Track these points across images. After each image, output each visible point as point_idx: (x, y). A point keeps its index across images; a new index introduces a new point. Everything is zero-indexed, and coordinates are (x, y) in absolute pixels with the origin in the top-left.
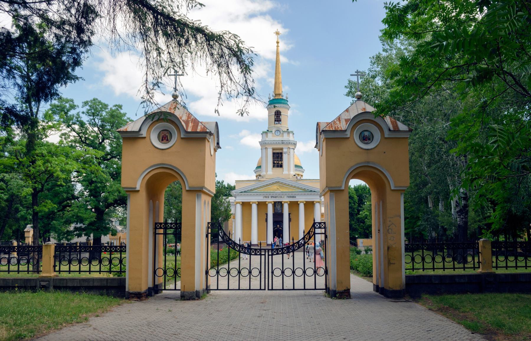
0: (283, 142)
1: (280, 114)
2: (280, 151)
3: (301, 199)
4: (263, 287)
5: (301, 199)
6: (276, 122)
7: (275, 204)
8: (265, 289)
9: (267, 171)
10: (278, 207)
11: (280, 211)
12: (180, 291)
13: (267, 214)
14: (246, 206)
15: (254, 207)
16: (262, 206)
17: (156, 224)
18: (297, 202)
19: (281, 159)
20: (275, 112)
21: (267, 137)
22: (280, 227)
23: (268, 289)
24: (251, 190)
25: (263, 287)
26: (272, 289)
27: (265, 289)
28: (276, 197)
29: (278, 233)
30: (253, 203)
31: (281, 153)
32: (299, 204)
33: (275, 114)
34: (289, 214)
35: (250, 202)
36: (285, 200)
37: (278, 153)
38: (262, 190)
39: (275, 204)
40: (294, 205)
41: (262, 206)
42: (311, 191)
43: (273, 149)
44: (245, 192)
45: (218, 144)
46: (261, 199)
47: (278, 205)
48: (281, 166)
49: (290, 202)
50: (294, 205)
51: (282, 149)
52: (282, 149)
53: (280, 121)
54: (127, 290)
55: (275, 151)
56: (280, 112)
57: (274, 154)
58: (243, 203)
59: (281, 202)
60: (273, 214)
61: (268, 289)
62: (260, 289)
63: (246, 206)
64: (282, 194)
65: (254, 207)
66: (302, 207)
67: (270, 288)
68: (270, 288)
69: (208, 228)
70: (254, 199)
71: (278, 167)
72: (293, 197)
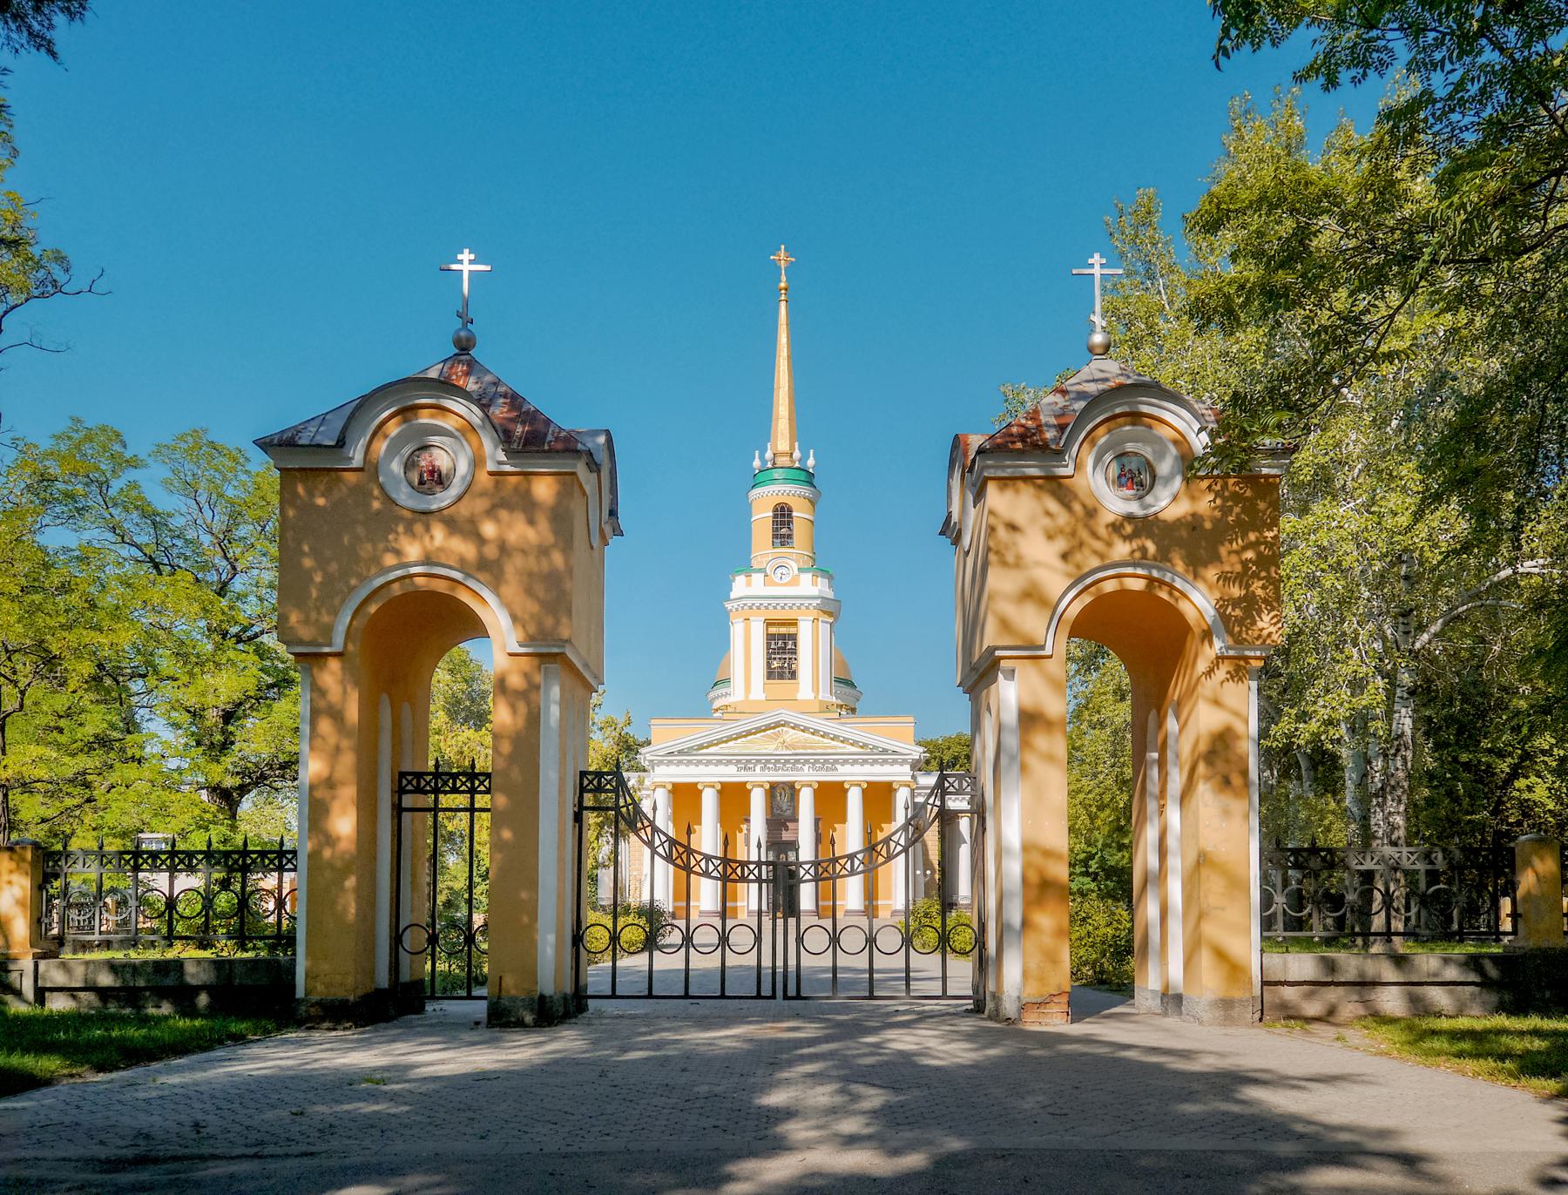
1: (790, 516)
2: (792, 630)
4: (766, 991)
5: (855, 774)
7: (773, 790)
8: (773, 997)
12: (484, 1004)
16: (733, 798)
17: (402, 775)
20: (775, 510)
21: (749, 584)
23: (786, 997)
24: (701, 747)
25: (766, 991)
26: (798, 997)
27: (773, 997)
31: (793, 637)
33: (775, 516)
34: (817, 821)
36: (806, 777)
37: (783, 637)
39: (773, 790)
40: (831, 798)
41: (733, 798)
42: (885, 751)
44: (680, 752)
45: (613, 513)
46: (731, 774)
47: (781, 800)
48: (793, 675)
50: (831, 798)
51: (793, 623)
52: (794, 623)
53: (790, 536)
54: (300, 993)
55: (773, 630)
56: (790, 510)
57: (770, 638)
58: (675, 785)
59: (791, 785)
61: (786, 997)
62: (759, 996)
66: (854, 800)
67: (792, 992)
68: (792, 992)
69: (583, 790)
70: (708, 775)
71: (781, 677)
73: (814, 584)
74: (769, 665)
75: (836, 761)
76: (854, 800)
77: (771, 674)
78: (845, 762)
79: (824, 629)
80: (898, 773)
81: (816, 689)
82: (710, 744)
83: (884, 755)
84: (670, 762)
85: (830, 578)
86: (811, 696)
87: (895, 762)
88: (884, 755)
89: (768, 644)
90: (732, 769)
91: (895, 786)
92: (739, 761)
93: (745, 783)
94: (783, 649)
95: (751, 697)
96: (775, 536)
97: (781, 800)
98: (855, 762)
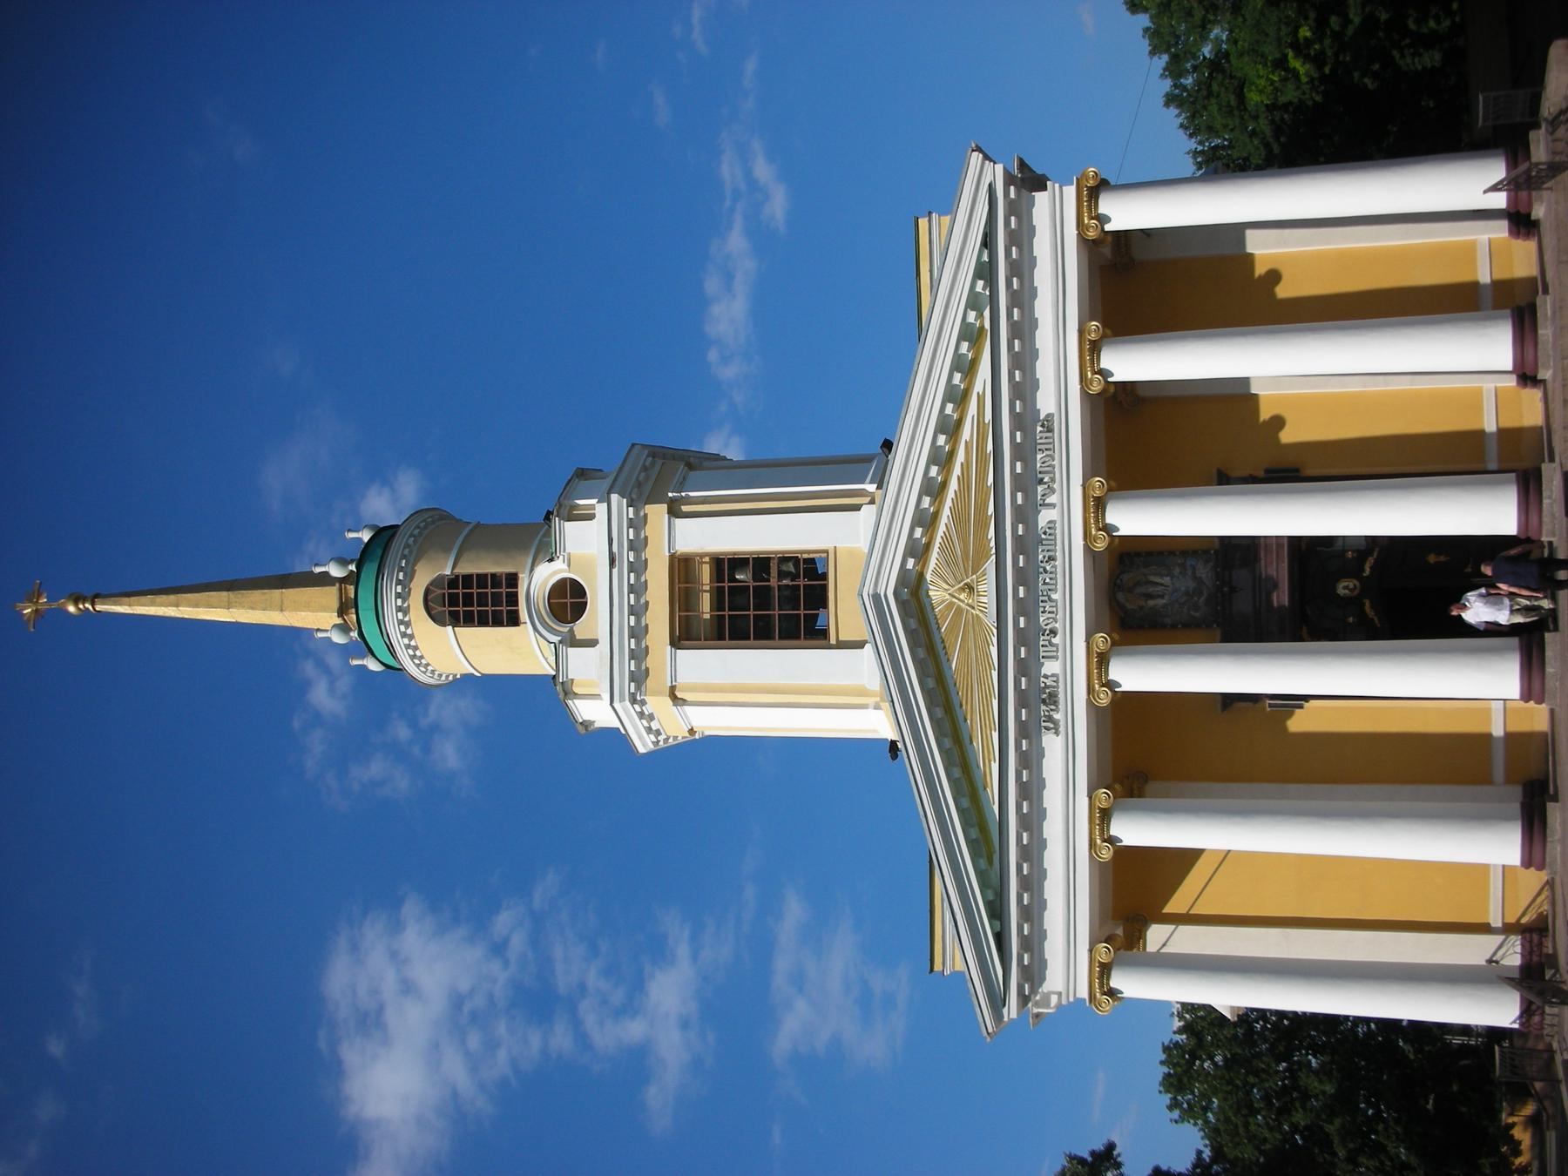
0: (630, 556)
1: (453, 582)
10: (1168, 586)
11: (1204, 571)
20: (437, 619)
22: (1356, 573)
29: (1405, 594)
31: (726, 565)
33: (456, 620)
38: (984, 744)
42: (986, 271)
43: (685, 635)
44: (997, 911)
46: (1066, 758)
47: (1146, 595)
51: (682, 567)
52: (682, 567)
75: (1018, 422)
78: (1025, 390)
84: (1027, 944)
85: (582, 474)
92: (1024, 730)
96: (498, 622)
97: (1146, 595)
98: (1025, 360)
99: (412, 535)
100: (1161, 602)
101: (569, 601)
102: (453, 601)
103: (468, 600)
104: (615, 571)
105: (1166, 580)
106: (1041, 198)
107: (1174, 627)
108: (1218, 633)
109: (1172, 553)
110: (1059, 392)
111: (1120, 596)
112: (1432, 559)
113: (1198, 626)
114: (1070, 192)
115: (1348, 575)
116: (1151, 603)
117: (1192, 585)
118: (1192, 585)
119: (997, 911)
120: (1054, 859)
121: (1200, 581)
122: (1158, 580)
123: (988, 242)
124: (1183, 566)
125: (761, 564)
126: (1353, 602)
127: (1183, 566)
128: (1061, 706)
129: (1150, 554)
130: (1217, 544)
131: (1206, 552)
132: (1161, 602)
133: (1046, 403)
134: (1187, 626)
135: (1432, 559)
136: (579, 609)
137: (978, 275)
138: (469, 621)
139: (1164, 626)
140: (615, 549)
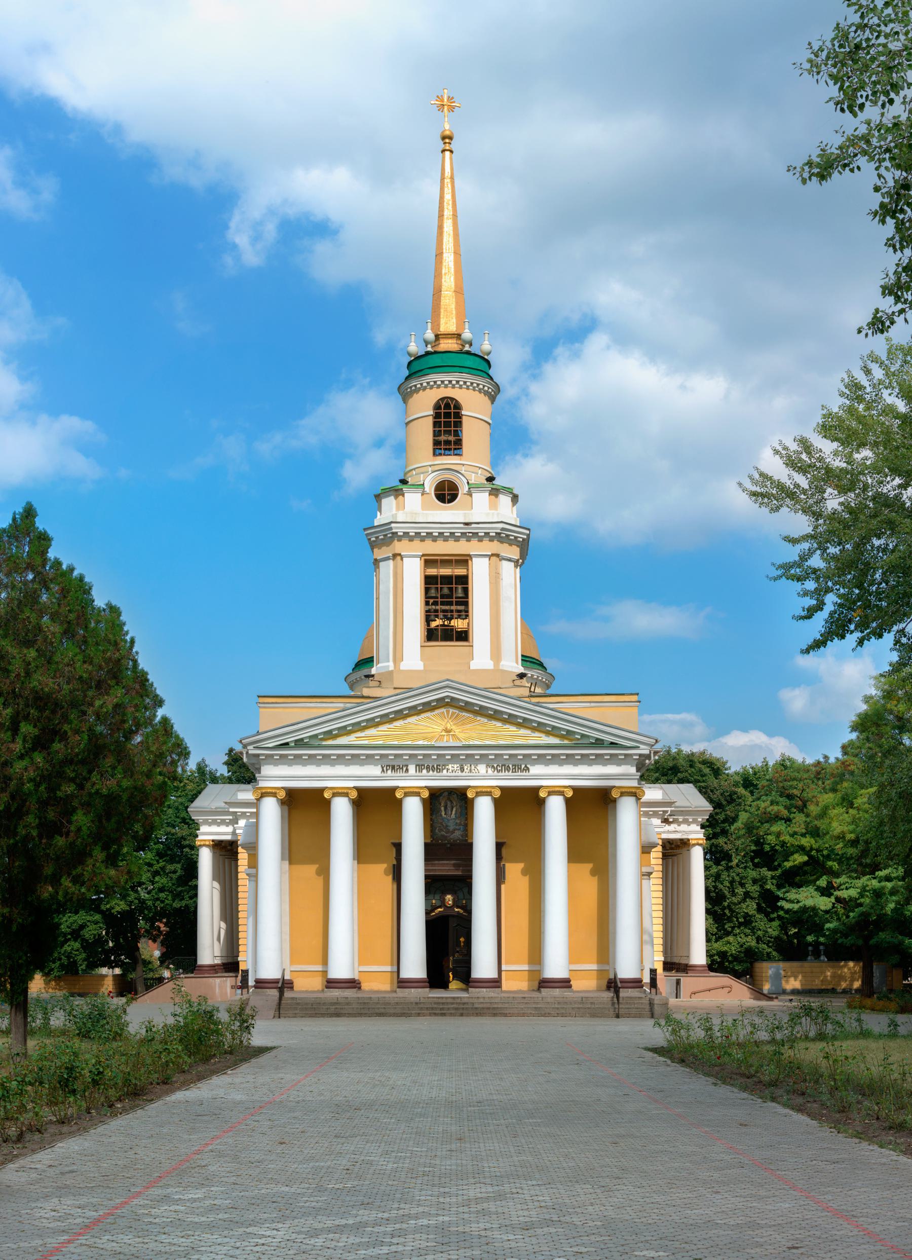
0: (470, 532)
1: (458, 416)
2: (460, 571)
3: (555, 777)
5: (555, 777)
6: (438, 452)
7: (435, 800)
9: (398, 657)
10: (450, 816)
11: (458, 834)
13: (398, 847)
14: (306, 806)
15: (342, 813)
16: (377, 807)
18: (537, 789)
19: (463, 606)
20: (437, 407)
22: (456, 904)
24: (329, 735)
28: (438, 769)
30: (338, 793)
31: (464, 580)
32: (541, 803)
33: (437, 416)
34: (499, 846)
35: (321, 790)
36: (482, 779)
37: (447, 579)
39: (435, 800)
40: (520, 808)
42: (599, 743)
43: (429, 562)
44: (300, 743)
46: (371, 776)
48: (463, 636)
49: (503, 789)
50: (520, 808)
51: (464, 561)
52: (464, 561)
53: (459, 443)
55: (432, 572)
56: (458, 406)
57: (429, 581)
60: (427, 846)
63: (306, 806)
64: (468, 756)
65: (342, 813)
66: (556, 812)
70: (339, 777)
72: (517, 768)
73: (493, 506)
74: (428, 620)
76: (556, 812)
77: (431, 635)
79: (509, 573)
80: (616, 773)
81: (496, 653)
82: (344, 731)
83: (598, 746)
86: (489, 665)
87: (613, 760)
88: (598, 746)
89: (427, 590)
90: (376, 770)
91: (615, 794)
93: (393, 790)
94: (447, 599)
95: (404, 666)
96: (436, 443)
99: (484, 386)
100: (443, 813)
101: (446, 493)
102: (448, 415)
103: (447, 424)
104: (462, 525)
105: (453, 816)
106: (632, 770)
107: (431, 820)
108: (429, 841)
109: (466, 819)
110: (541, 776)
111: (446, 794)
112: (462, 939)
113: (432, 831)
114: (634, 783)
115: (454, 900)
116: (443, 809)
117: (451, 828)
118: (451, 828)
119: (300, 743)
120: (325, 770)
121: (453, 832)
122: (454, 812)
123: (613, 745)
124: (460, 824)
125: (465, 601)
126: (443, 904)
127: (460, 824)
128: (393, 774)
129: (466, 808)
130: (469, 841)
131: (467, 836)
132: (443, 813)
133: (535, 770)
134: (432, 826)
135: (462, 939)
136: (441, 498)
137: (597, 739)
138: (435, 424)
139: (431, 815)
140: (473, 526)
